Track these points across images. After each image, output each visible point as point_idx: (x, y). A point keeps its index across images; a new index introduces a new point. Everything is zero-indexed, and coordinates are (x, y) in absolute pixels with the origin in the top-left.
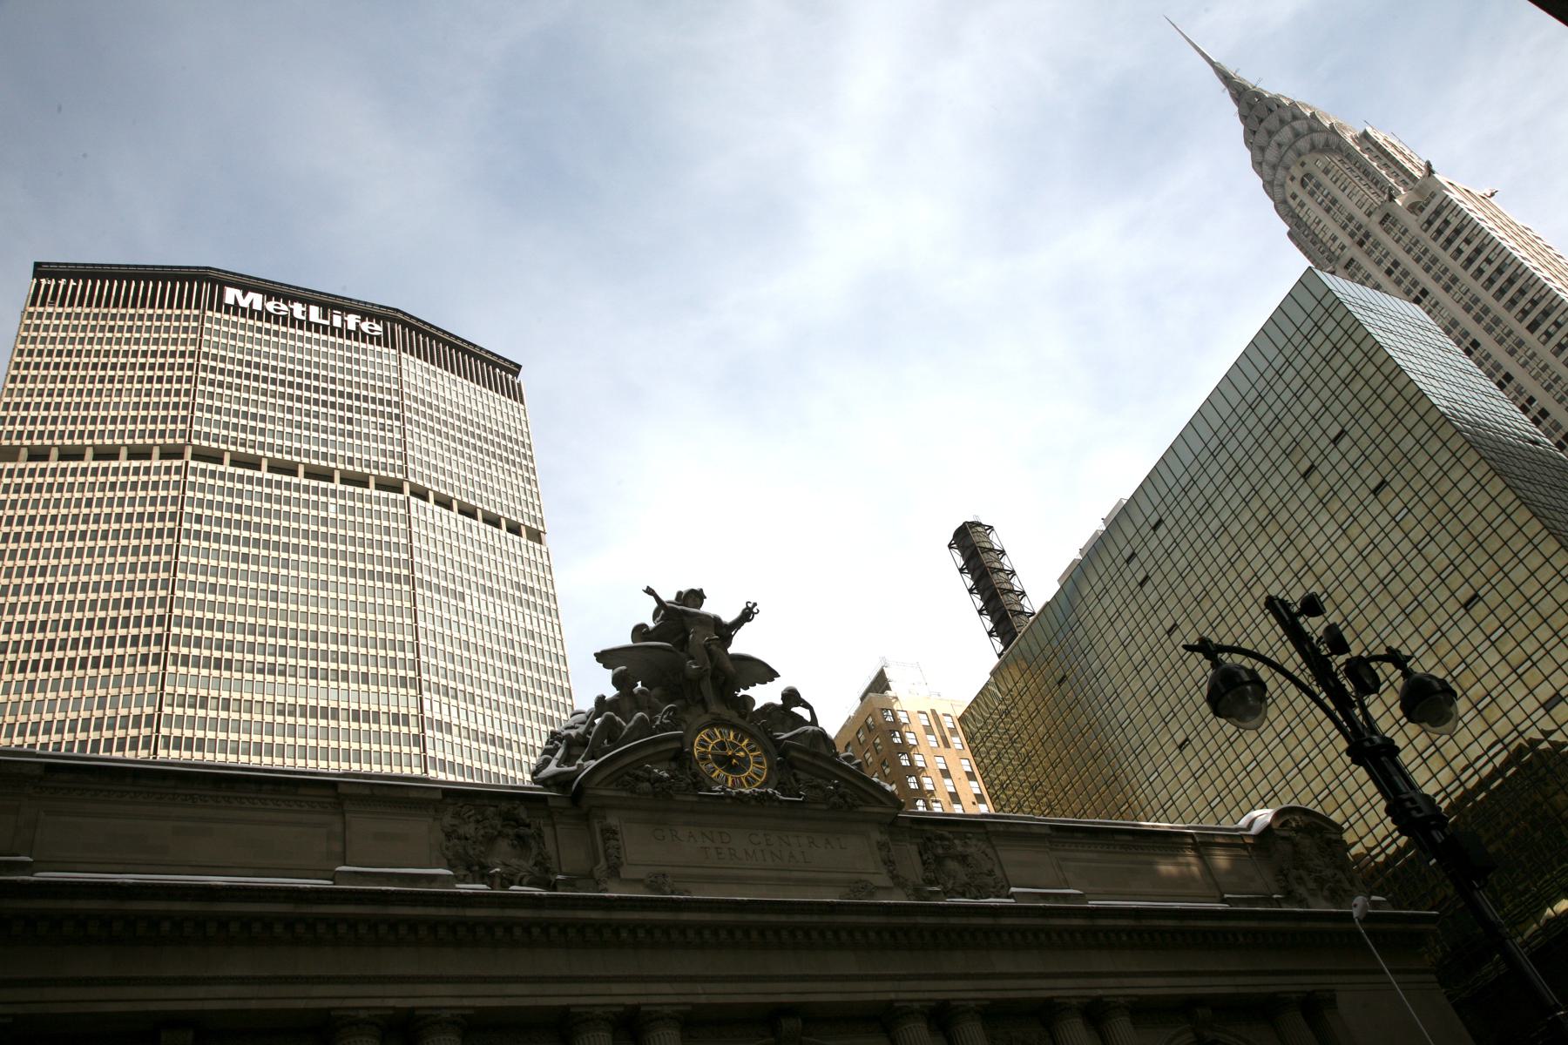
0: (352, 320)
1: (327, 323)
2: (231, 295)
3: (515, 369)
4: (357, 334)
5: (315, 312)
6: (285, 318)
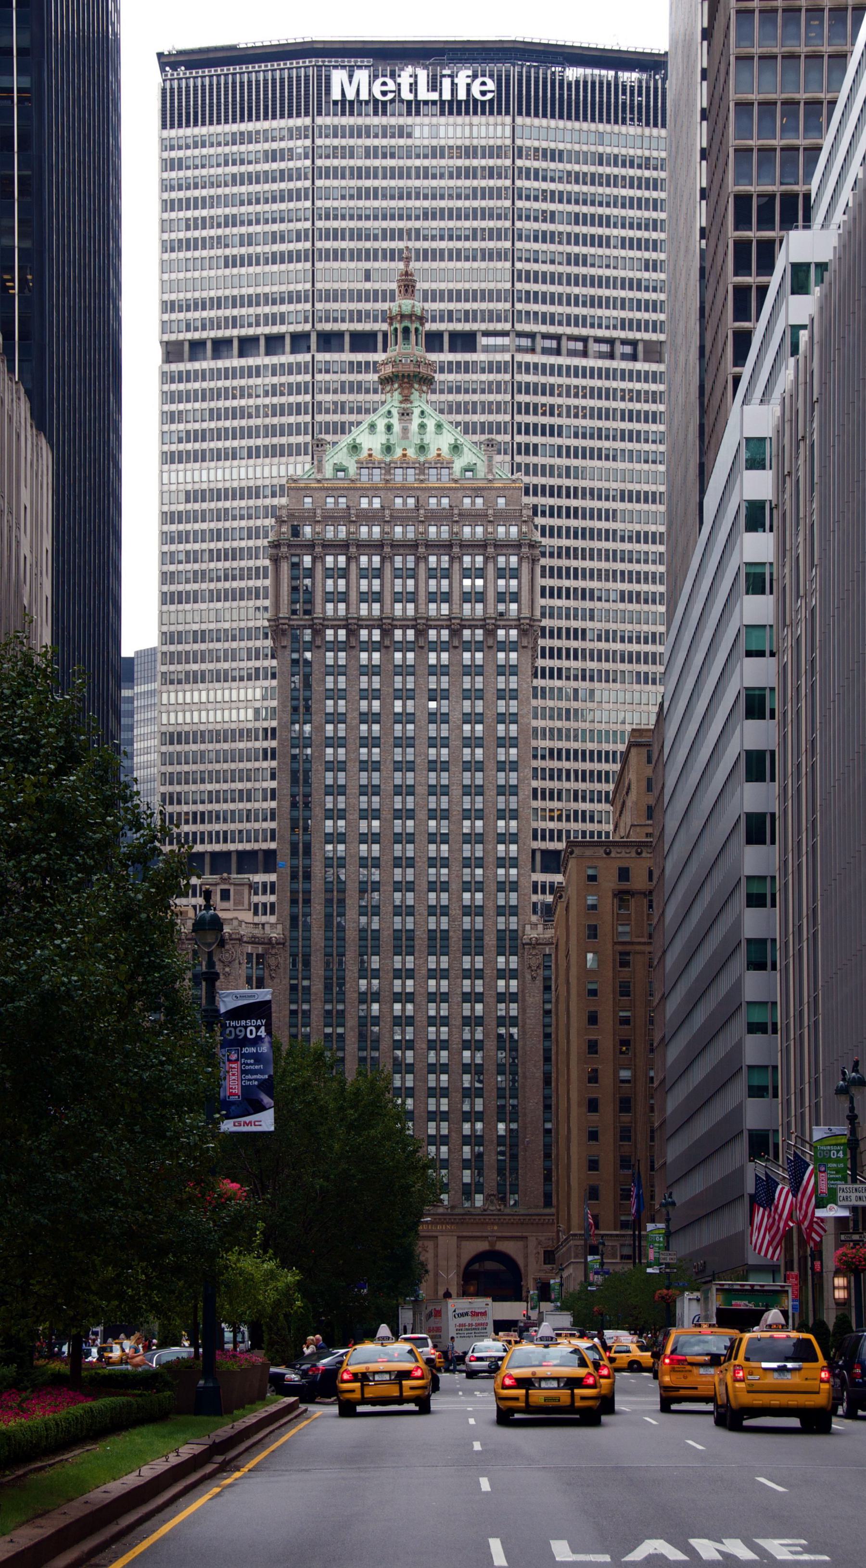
0: (463, 77)
1: (434, 96)
5: (423, 75)
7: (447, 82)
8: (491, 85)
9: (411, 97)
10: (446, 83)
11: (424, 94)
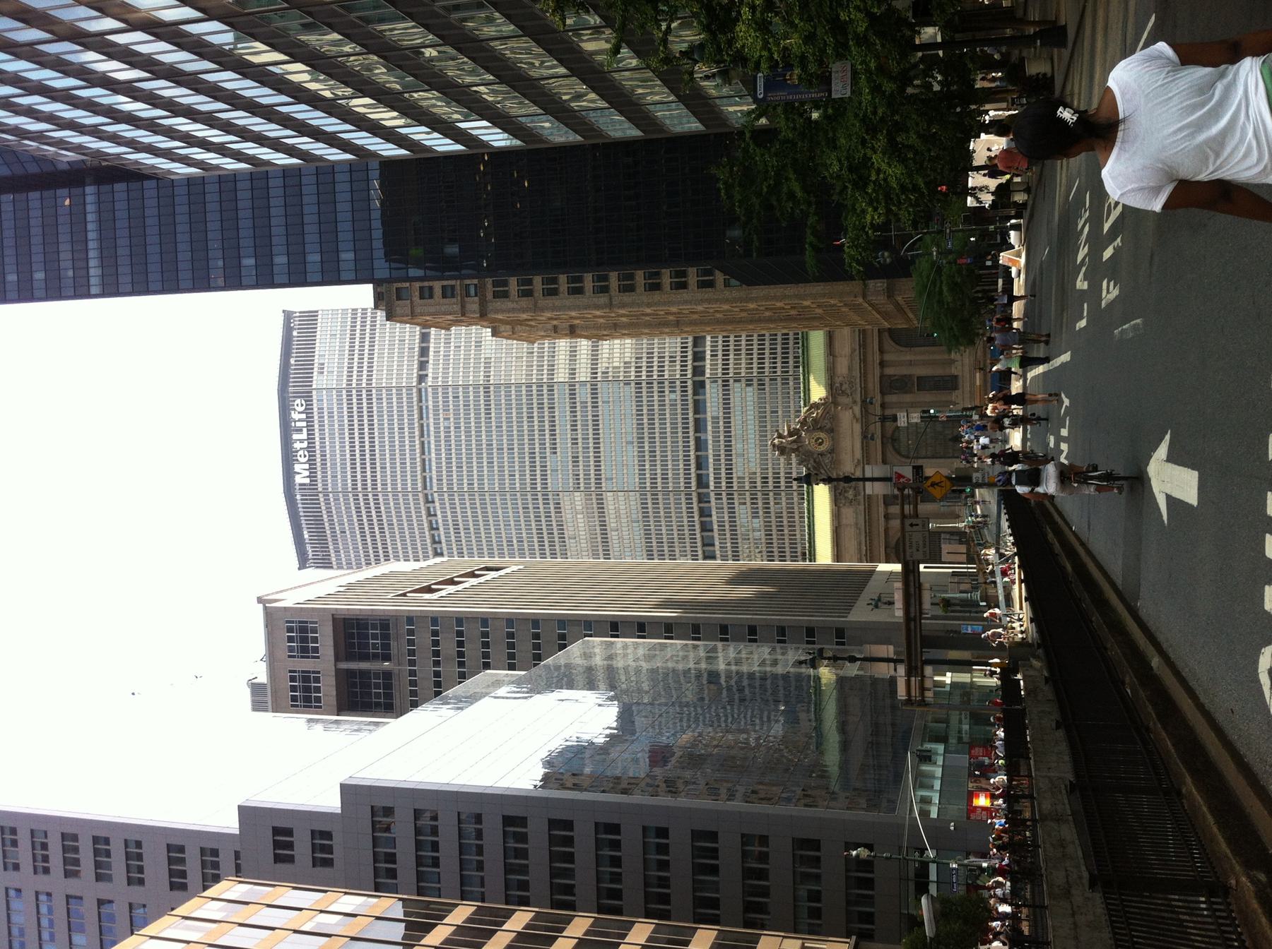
0: (295, 416)
2: (299, 479)
4: (308, 411)
5: (295, 436)
7: (298, 424)
8: (298, 401)
10: (298, 424)
11: (304, 436)
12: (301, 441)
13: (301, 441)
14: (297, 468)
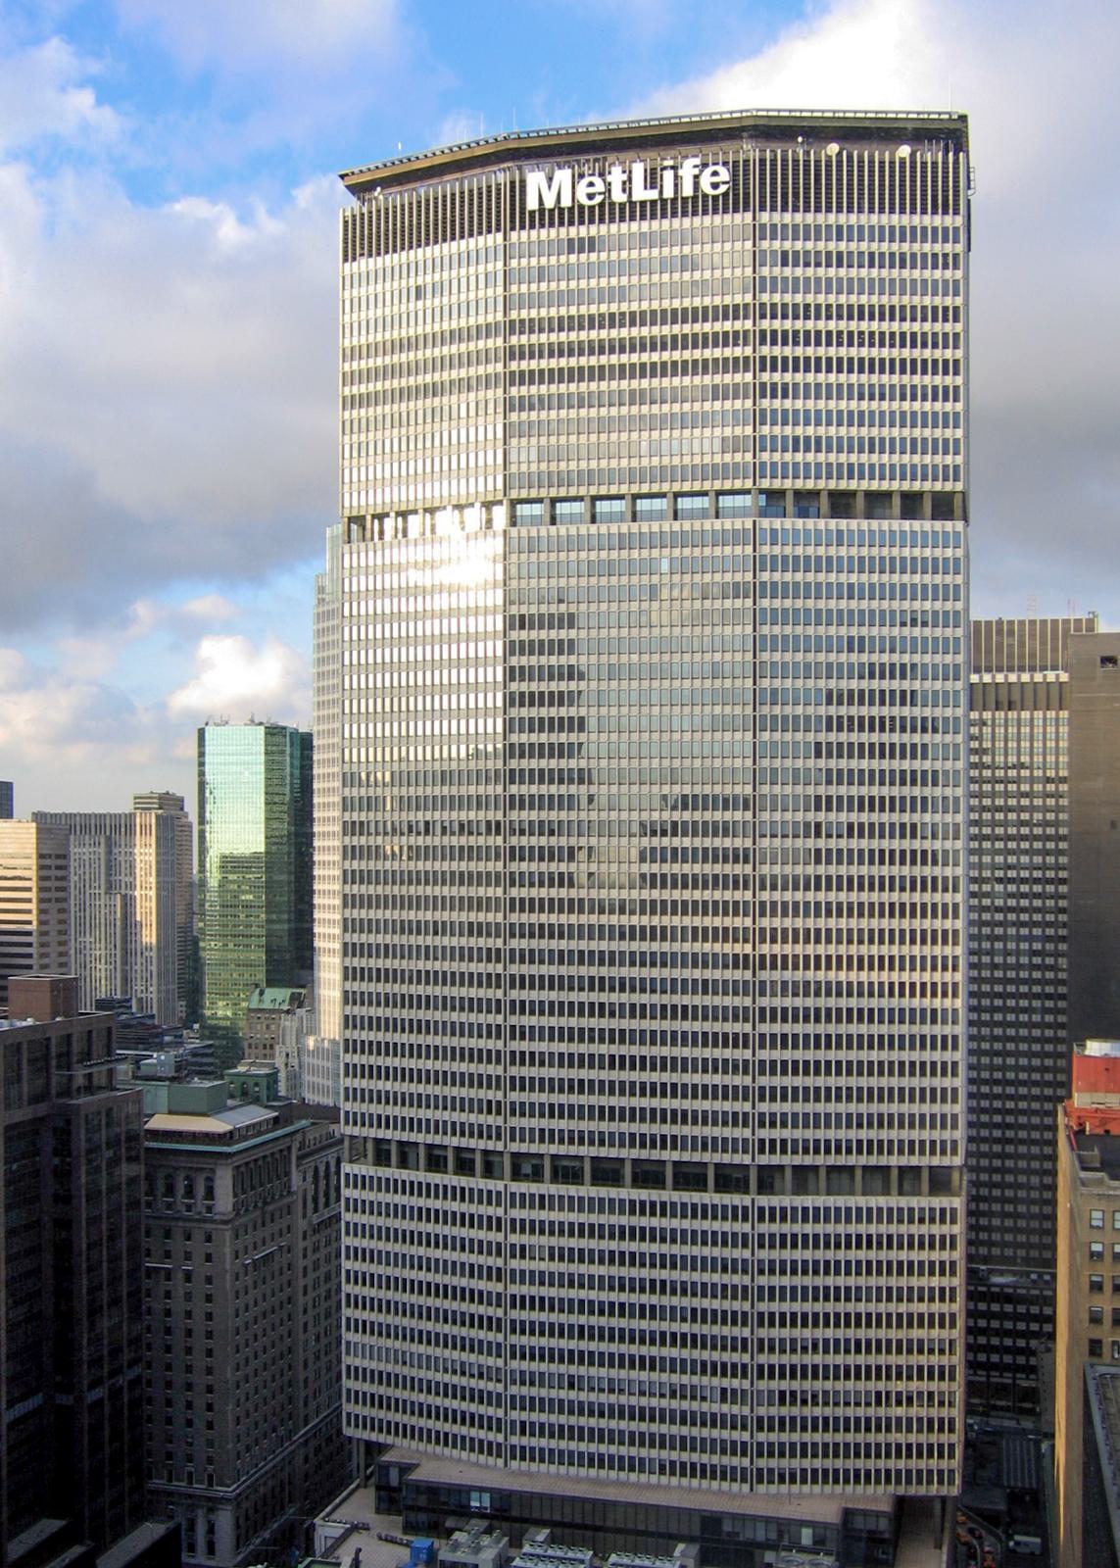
1: (653, 194)
2: (535, 179)
3: (951, 134)
4: (697, 204)
5: (638, 170)
6: (601, 205)
7: (668, 175)
8: (725, 175)
9: (623, 198)
10: (668, 175)
11: (641, 193)
12: (627, 186)
13: (627, 186)
14: (563, 176)
